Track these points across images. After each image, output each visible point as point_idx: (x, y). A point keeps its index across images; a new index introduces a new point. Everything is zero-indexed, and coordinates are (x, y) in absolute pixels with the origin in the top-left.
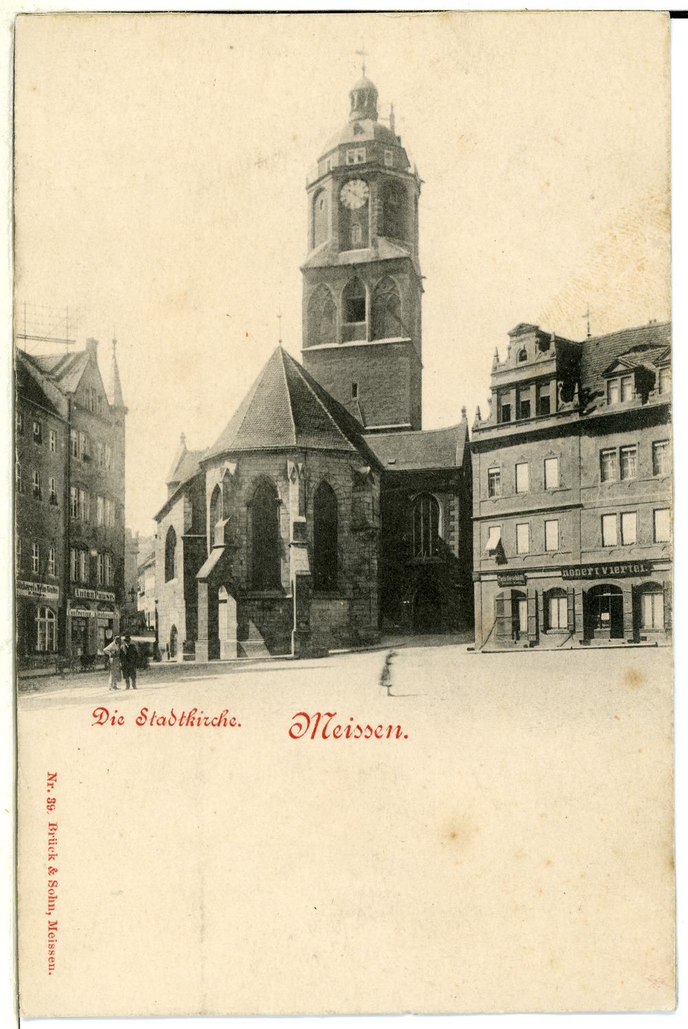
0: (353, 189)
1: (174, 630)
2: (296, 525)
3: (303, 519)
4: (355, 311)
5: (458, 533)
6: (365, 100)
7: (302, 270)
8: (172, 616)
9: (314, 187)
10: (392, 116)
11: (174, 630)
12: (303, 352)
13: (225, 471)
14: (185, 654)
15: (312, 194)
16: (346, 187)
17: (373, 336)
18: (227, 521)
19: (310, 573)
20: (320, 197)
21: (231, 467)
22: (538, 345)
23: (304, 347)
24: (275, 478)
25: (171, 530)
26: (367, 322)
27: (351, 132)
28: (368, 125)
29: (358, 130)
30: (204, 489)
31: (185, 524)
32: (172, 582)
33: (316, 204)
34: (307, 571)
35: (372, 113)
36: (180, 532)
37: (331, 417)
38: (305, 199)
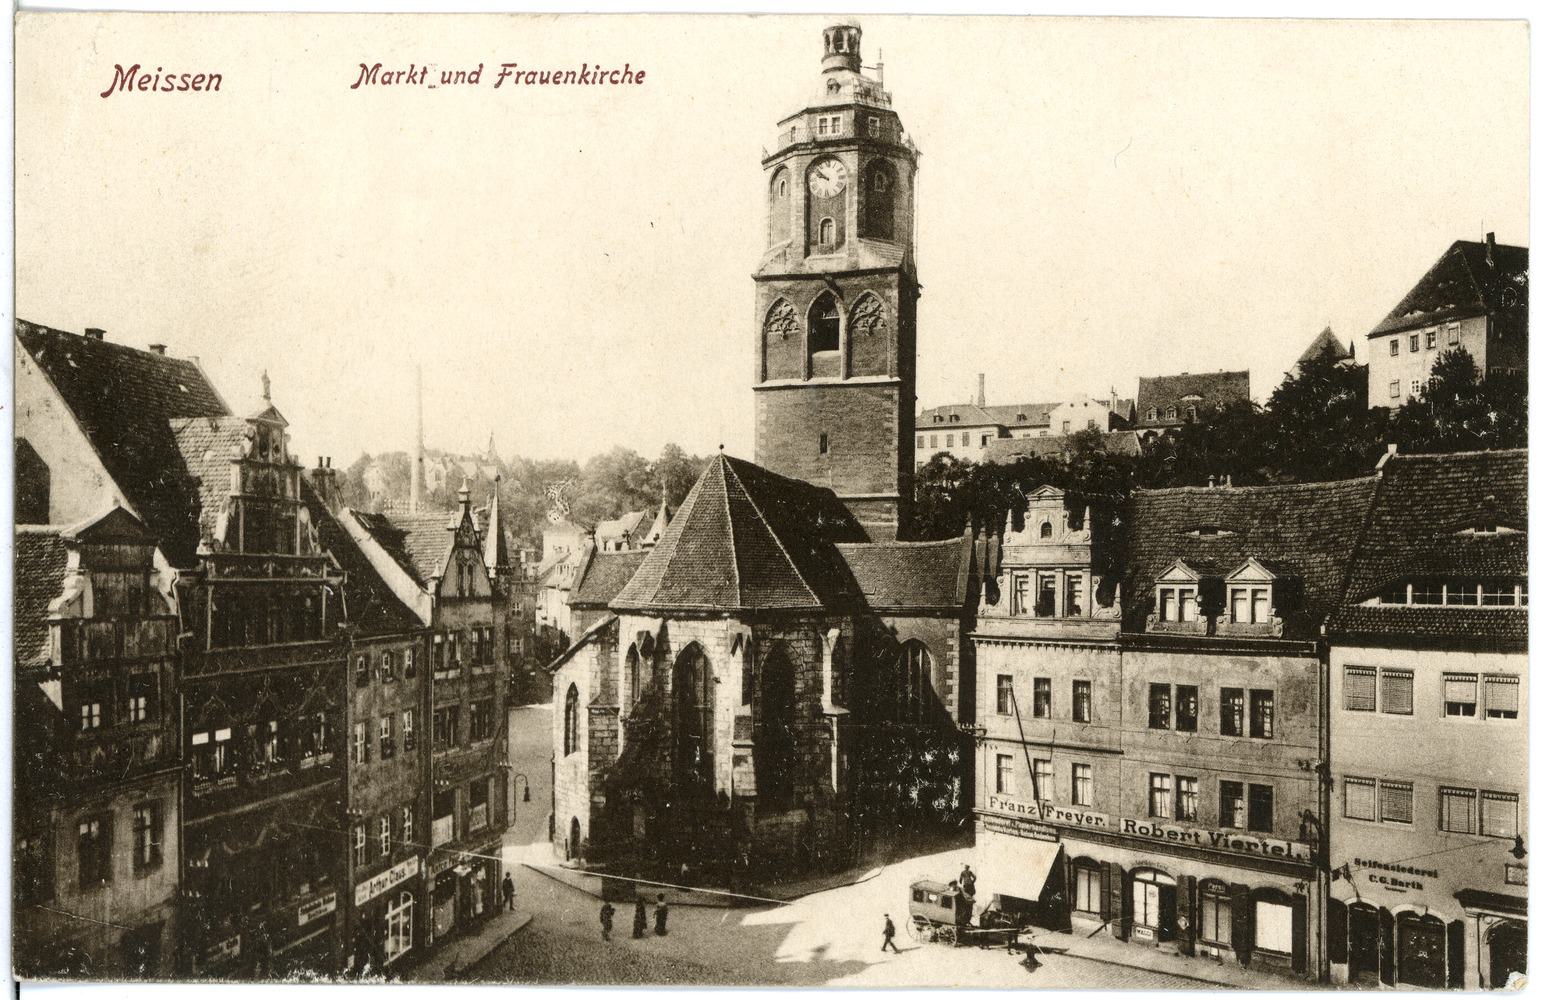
0: (824, 172)
1: (575, 822)
3: (747, 711)
4: (823, 336)
5: (957, 697)
6: (844, 45)
8: (572, 804)
9: (774, 162)
10: (880, 66)
11: (575, 822)
13: (645, 634)
15: (772, 170)
17: (848, 375)
19: (754, 793)
20: (781, 178)
21: (652, 626)
22: (1066, 520)
24: (711, 648)
25: (573, 692)
26: (841, 352)
27: (823, 88)
29: (834, 87)
30: (617, 641)
31: (591, 686)
32: (573, 756)
33: (776, 183)
34: (750, 790)
35: (854, 63)
36: (584, 699)
37: (788, 556)
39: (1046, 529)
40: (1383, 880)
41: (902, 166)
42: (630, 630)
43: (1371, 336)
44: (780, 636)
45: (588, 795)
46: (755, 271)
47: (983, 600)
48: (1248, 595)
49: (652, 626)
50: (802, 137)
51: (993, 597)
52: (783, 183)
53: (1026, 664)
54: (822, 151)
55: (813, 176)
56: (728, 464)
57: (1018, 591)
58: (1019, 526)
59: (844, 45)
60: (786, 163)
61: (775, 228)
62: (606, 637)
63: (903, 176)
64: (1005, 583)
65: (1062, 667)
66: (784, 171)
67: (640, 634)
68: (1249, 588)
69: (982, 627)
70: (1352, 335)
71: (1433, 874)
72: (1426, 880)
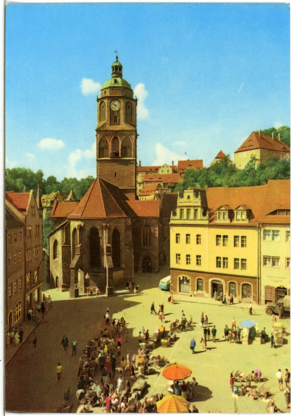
2: (107, 247)
3: (109, 245)
7: (96, 130)
9: (101, 100)
12: (97, 160)
14: (63, 289)
15: (100, 102)
16: (112, 102)
18: (81, 244)
19: (113, 267)
23: (97, 158)
27: (113, 82)
28: (119, 79)
29: (116, 81)
30: (70, 228)
33: (101, 106)
35: (120, 75)
38: (97, 104)
39: (189, 197)
40: (273, 280)
41: (133, 103)
42: (74, 225)
43: (235, 153)
44: (116, 225)
45: (62, 270)
46: (96, 129)
47: (172, 215)
48: (240, 213)
49: (82, 224)
50: (108, 94)
51: (175, 214)
52: (103, 106)
53: (183, 231)
54: (112, 99)
55: (111, 104)
56: (101, 181)
57: (181, 213)
58: (182, 196)
59: (117, 70)
60: (104, 100)
61: (101, 117)
62: (66, 228)
63: (134, 106)
64: (178, 211)
65: (193, 232)
66: (103, 103)
67: (78, 226)
68: (240, 212)
69: (172, 222)
70: (229, 151)
71: (285, 278)
72: (283, 280)
